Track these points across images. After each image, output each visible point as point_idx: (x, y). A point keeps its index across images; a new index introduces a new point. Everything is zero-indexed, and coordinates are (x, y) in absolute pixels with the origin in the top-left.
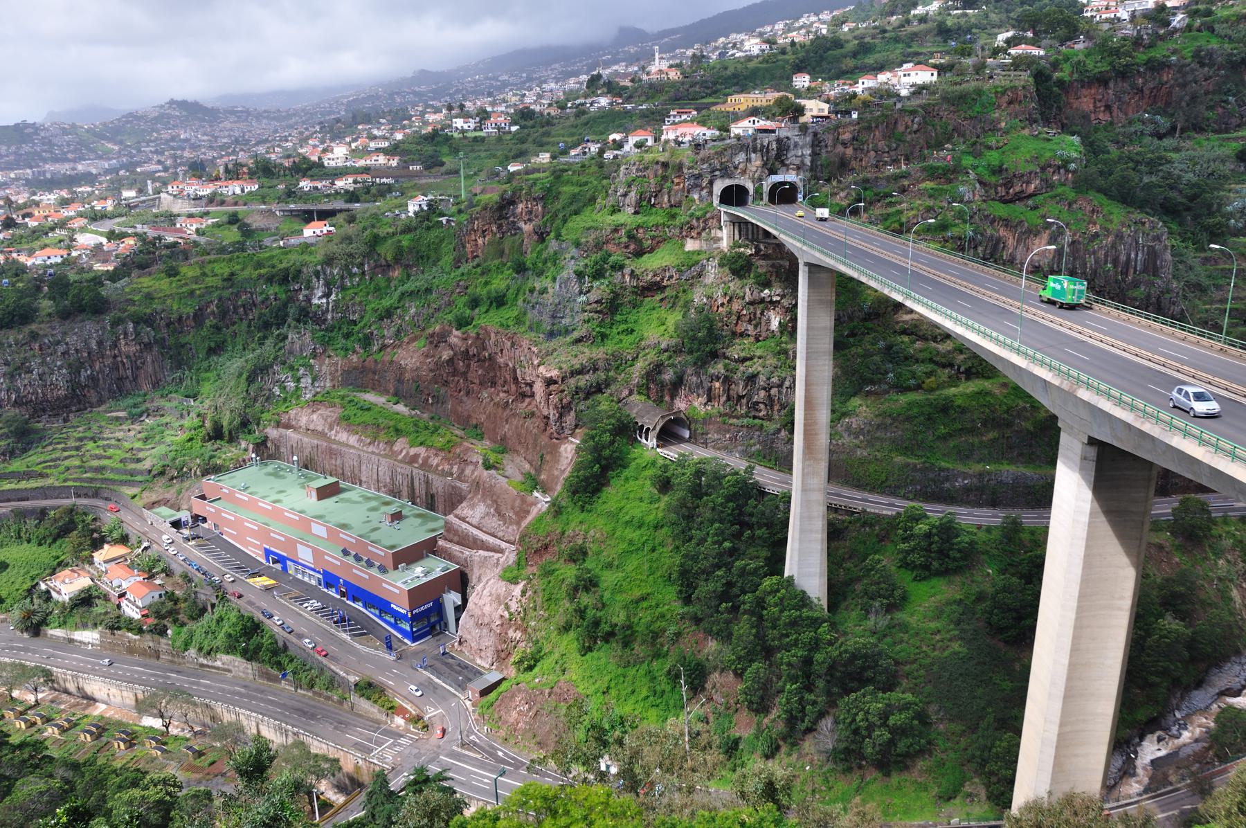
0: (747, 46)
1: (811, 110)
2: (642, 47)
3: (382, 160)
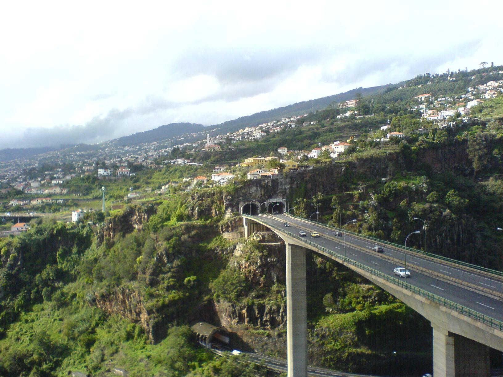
0: (254, 134)
1: (289, 166)
2: (200, 134)
3: (58, 190)
